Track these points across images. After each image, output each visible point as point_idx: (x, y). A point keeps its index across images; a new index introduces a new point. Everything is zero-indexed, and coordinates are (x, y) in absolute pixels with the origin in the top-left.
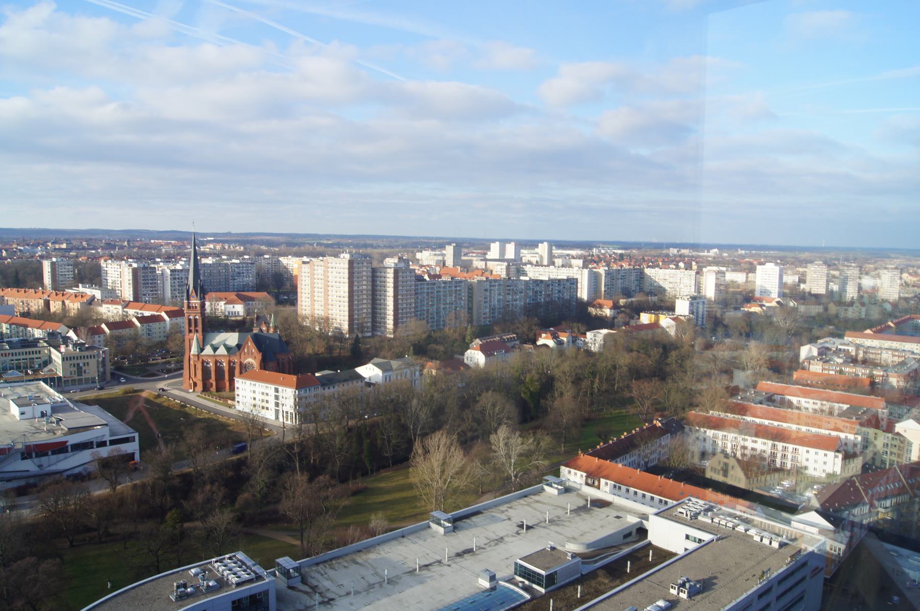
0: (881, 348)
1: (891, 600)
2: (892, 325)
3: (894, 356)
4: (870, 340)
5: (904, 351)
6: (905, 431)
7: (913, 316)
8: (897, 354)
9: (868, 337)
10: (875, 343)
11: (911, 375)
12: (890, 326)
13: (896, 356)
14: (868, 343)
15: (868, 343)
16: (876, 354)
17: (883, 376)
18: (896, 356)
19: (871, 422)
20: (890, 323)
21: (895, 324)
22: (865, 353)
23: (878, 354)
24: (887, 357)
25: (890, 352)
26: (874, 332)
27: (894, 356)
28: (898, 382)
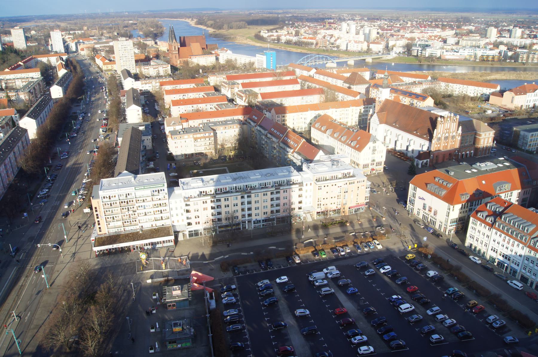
0: (14, 79)
1: (23, 216)
2: (22, 64)
3: (22, 82)
4: (8, 75)
5: (27, 78)
6: (25, 124)
7: (34, 56)
8: (24, 80)
9: (7, 73)
10: (12, 76)
11: (31, 91)
12: (20, 65)
13: (24, 82)
14: (8, 77)
15: (8, 77)
16: (12, 83)
17: (15, 95)
18: (24, 82)
19: (8, 124)
20: (20, 63)
21: (23, 63)
22: (6, 83)
23: (13, 83)
24: (19, 84)
25: (20, 80)
26: (11, 70)
27: (22, 82)
28: (25, 97)
